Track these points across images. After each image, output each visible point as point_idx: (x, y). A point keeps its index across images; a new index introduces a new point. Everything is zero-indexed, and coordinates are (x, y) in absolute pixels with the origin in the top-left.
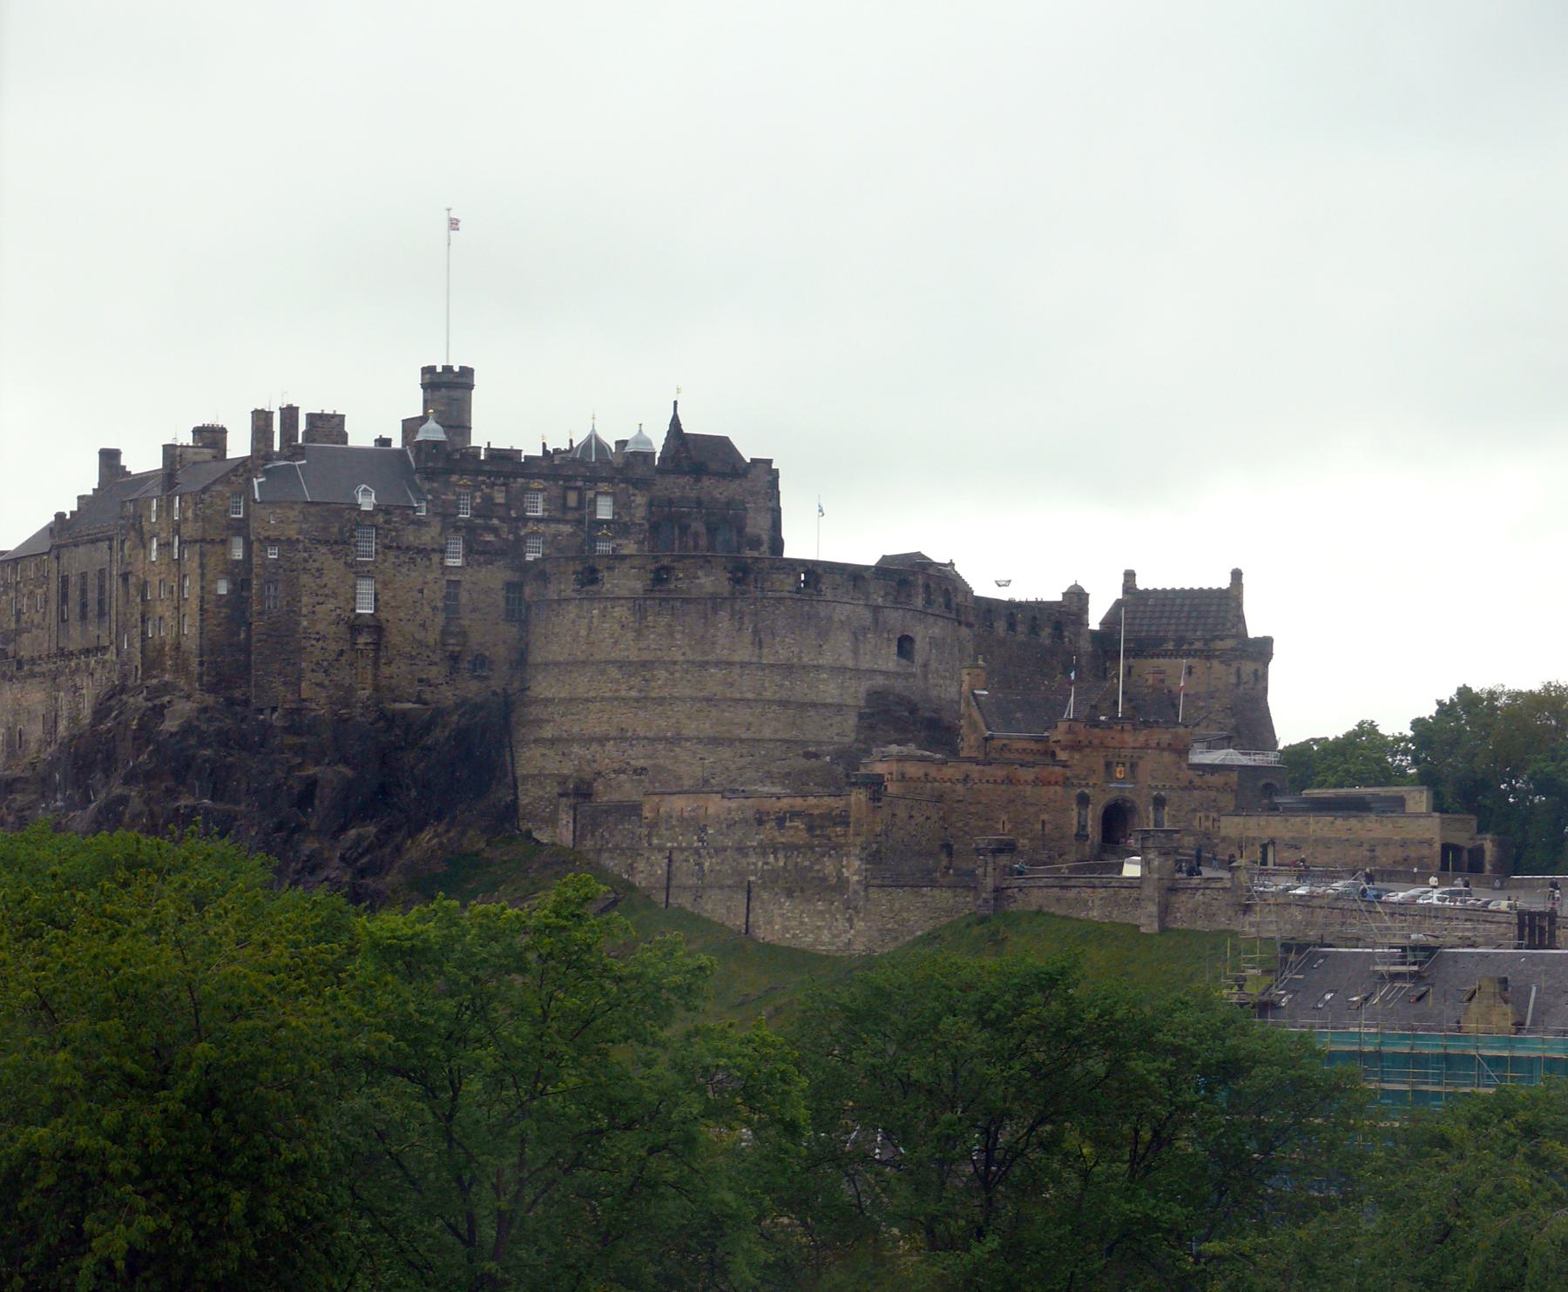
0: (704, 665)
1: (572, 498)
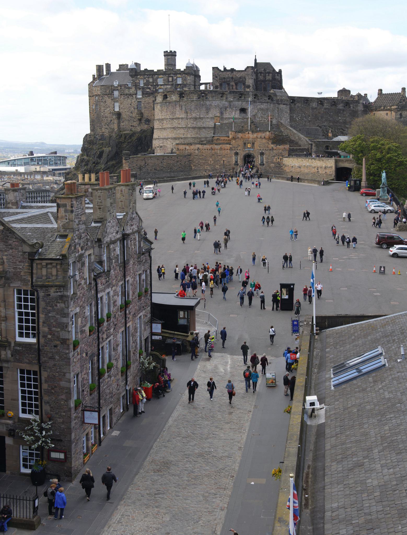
0: (173, 119)
1: (170, 79)
